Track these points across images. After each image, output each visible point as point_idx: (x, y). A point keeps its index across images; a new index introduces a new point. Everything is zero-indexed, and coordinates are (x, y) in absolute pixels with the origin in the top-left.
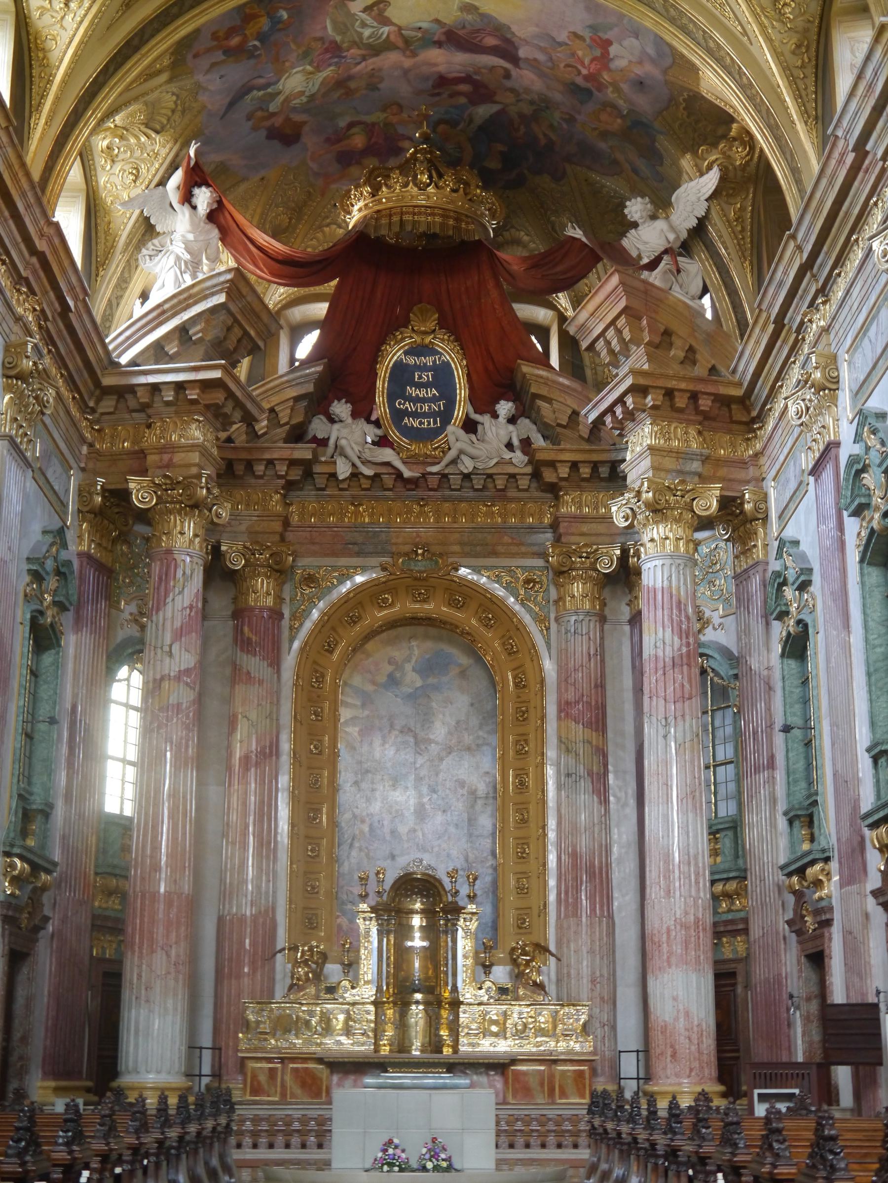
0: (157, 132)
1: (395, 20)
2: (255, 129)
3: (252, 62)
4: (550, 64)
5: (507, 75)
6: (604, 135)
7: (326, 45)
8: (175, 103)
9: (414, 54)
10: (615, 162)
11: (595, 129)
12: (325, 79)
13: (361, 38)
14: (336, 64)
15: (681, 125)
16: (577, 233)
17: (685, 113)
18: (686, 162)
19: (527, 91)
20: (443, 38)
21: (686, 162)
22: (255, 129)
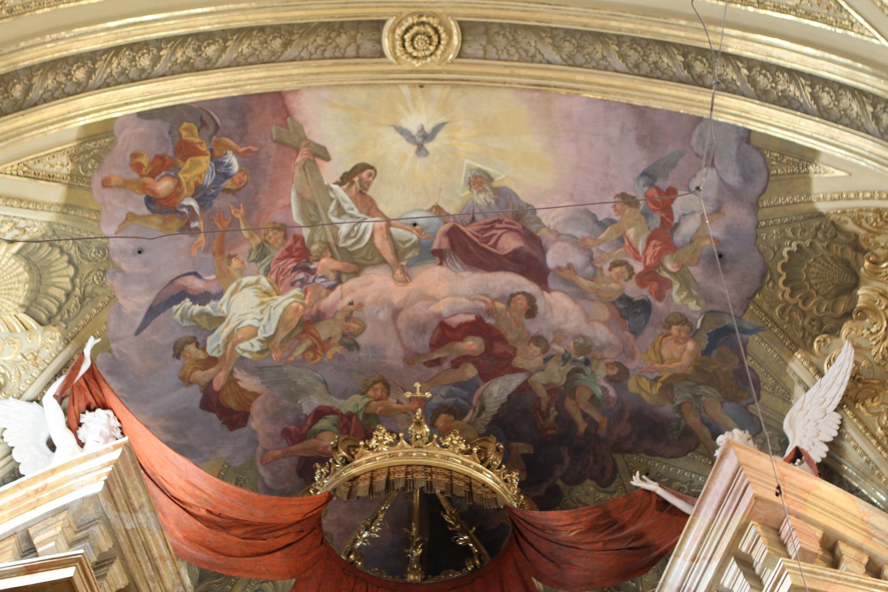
0: (40, 323)
1: (381, 207)
2: (186, 380)
3: (186, 238)
4: (590, 269)
5: (531, 312)
6: (668, 387)
7: (290, 242)
8: (72, 281)
9: (407, 279)
10: (688, 432)
11: (656, 380)
12: (285, 310)
13: (336, 238)
14: (303, 282)
15: (783, 310)
16: (652, 486)
17: (788, 290)
18: (797, 365)
19: (559, 334)
20: (445, 244)
21: (797, 365)
22: (186, 380)
